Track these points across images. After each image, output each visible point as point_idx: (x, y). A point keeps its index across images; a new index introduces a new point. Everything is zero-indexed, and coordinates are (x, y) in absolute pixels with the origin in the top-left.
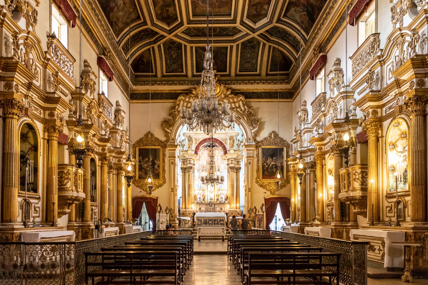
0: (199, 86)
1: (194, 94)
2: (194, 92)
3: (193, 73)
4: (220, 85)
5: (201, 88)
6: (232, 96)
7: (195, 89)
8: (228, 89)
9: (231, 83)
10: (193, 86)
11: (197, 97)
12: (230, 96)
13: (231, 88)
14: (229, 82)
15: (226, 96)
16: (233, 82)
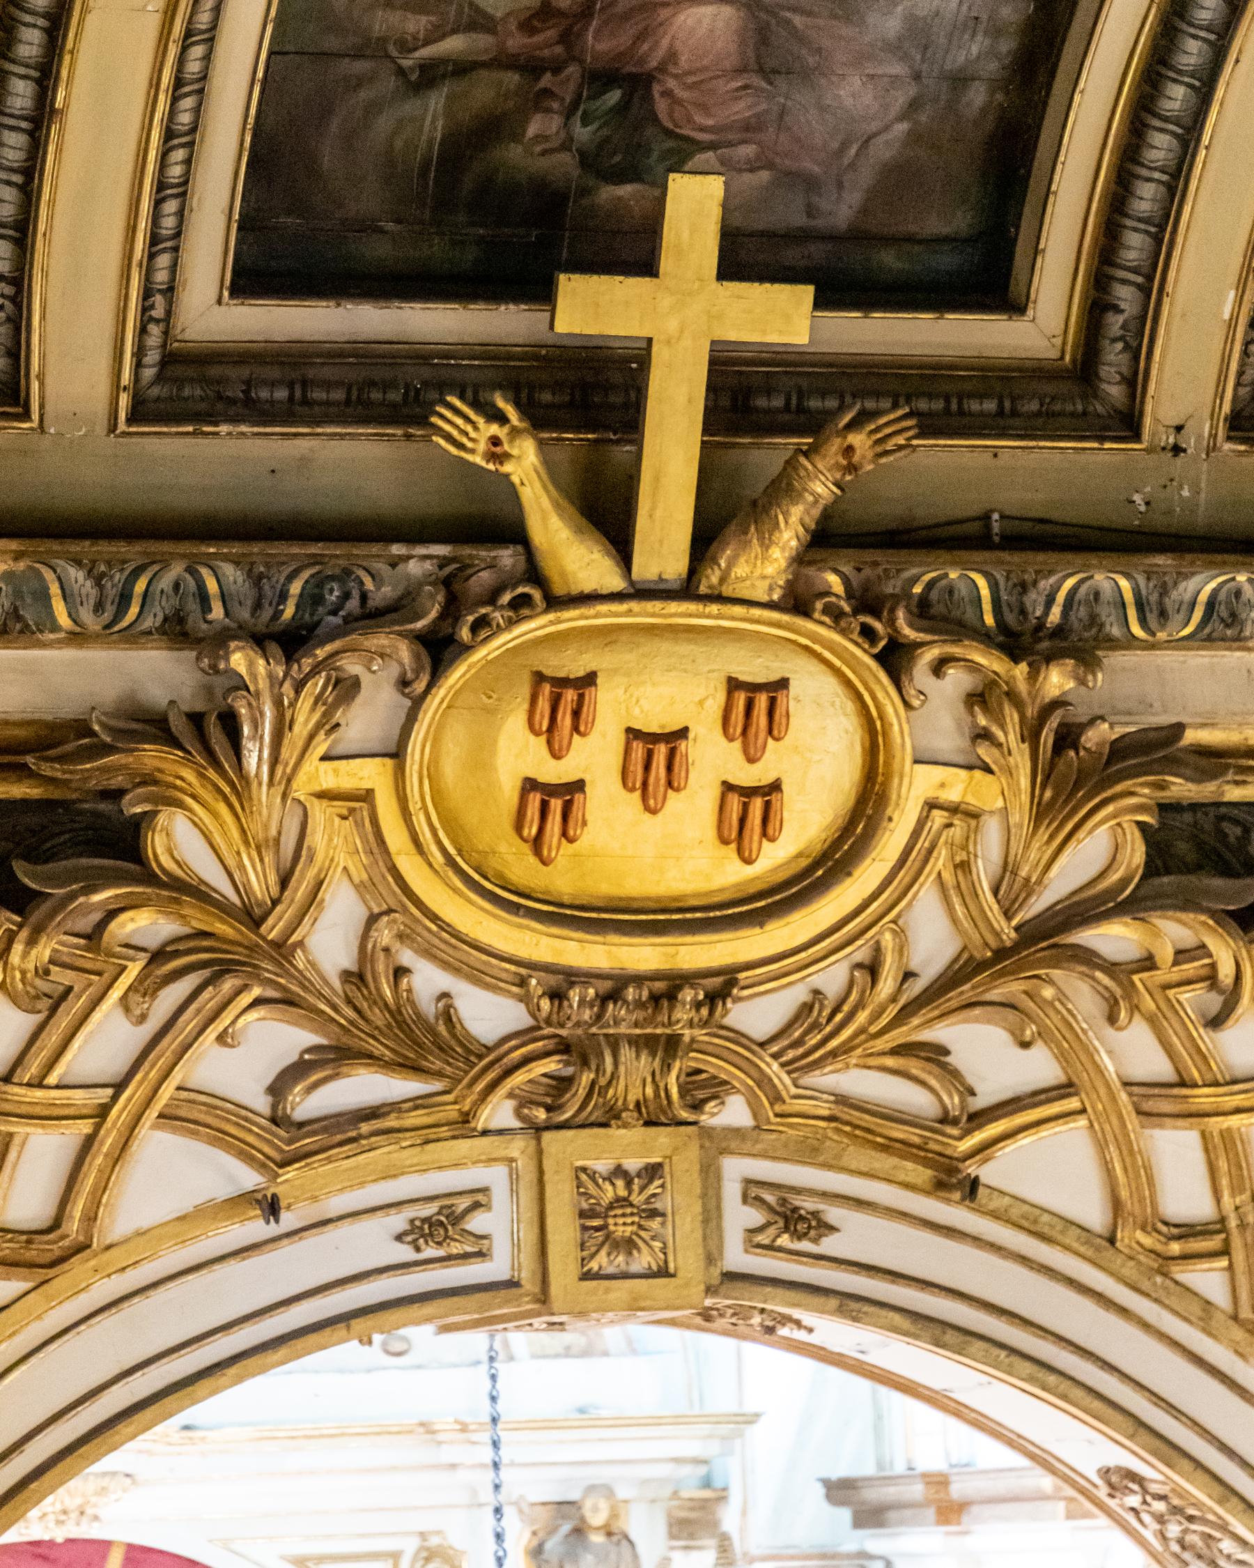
0: (347, 689)
1: (183, 889)
2: (180, 840)
3: (159, 295)
4: (895, 659)
5: (369, 716)
6: (1174, 930)
7: (211, 731)
8: (1073, 772)
9: (1154, 610)
10: (159, 674)
11: (236, 949)
12: (1114, 938)
13: (1155, 749)
14: (1116, 582)
15: (1028, 947)
16: (1204, 584)
